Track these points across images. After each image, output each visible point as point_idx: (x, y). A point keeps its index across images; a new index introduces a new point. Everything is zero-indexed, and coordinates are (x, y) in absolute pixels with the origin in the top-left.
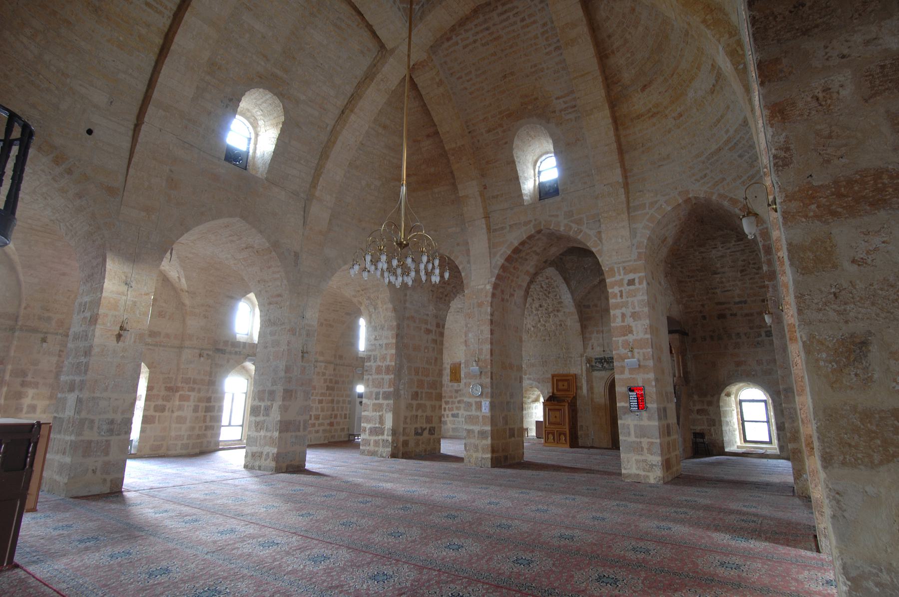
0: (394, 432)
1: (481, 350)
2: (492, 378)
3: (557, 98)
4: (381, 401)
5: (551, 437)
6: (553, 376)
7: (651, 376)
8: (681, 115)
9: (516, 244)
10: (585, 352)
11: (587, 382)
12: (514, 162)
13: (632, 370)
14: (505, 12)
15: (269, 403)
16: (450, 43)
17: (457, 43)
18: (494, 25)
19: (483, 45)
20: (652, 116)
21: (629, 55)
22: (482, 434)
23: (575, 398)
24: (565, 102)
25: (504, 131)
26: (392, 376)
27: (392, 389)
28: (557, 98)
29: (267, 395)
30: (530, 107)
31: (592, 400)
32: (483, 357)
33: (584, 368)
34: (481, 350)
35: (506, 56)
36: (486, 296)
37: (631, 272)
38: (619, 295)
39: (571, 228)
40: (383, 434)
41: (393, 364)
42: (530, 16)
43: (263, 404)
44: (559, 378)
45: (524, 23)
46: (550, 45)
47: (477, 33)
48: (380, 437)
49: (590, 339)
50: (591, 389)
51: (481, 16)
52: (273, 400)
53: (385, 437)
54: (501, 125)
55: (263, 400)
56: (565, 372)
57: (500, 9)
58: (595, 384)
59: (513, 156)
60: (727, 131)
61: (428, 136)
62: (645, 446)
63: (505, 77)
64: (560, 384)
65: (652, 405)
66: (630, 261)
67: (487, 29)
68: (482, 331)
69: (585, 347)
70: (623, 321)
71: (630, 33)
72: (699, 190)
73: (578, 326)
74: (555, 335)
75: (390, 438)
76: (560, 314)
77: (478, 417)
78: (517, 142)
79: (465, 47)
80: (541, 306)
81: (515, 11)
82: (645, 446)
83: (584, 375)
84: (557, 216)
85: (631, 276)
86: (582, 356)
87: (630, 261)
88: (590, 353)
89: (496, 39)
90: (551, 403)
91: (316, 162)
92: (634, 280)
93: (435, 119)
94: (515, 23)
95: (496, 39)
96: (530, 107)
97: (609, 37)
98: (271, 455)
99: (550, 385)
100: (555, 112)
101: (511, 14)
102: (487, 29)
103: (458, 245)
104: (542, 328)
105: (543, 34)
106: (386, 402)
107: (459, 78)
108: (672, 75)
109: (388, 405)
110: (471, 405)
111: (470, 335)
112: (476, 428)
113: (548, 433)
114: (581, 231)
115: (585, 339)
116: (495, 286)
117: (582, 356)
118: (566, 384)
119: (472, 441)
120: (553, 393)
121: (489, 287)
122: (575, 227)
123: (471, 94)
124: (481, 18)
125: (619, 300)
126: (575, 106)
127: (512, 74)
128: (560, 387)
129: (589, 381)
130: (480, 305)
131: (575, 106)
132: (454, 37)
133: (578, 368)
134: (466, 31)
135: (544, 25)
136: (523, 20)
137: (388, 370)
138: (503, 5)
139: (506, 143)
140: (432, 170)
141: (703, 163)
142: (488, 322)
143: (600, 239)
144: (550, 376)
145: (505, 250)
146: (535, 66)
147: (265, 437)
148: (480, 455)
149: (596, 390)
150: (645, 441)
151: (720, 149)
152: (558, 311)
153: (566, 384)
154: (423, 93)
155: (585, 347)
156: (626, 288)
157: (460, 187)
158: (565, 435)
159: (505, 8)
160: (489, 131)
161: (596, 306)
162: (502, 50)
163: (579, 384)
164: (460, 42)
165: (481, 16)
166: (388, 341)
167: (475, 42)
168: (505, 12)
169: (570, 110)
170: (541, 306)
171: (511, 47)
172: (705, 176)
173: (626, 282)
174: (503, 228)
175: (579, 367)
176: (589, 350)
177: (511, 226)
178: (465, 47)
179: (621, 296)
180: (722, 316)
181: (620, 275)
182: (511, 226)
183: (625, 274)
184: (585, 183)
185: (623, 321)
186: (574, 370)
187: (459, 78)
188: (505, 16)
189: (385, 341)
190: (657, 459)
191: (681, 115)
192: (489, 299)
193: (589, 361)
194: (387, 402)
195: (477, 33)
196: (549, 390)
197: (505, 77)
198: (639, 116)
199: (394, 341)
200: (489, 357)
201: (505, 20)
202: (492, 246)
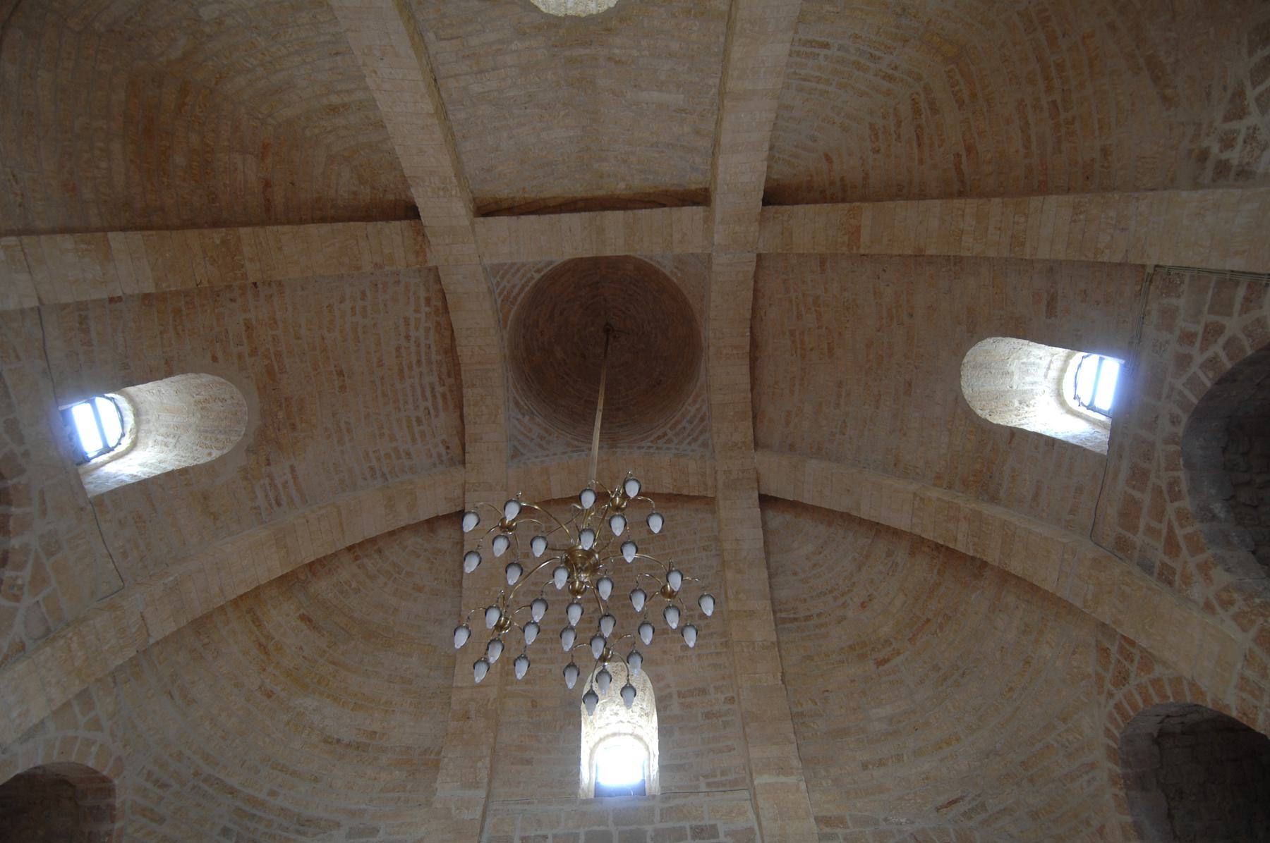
3: (292, 468)
8: (270, 695)
12: (169, 374)
14: (434, 397)
16: (422, 302)
17: (417, 311)
18: (421, 374)
19: (398, 349)
20: (260, 645)
21: (354, 585)
24: (285, 483)
25: (240, 356)
28: (292, 468)
30: (281, 415)
35: (373, 382)
39: (20, 567)
42: (423, 434)
45: (415, 423)
46: (379, 459)
47: (418, 346)
51: (439, 358)
54: (254, 352)
57: (439, 389)
59: (183, 371)
60: (273, 793)
61: (267, 184)
63: (341, 374)
67: (419, 362)
71: (385, 584)
72: (125, 795)
78: (206, 378)
79: (407, 320)
81: (432, 411)
84: (44, 513)
89: (401, 371)
93: (312, 229)
94: (417, 407)
95: (401, 371)
96: (281, 415)
97: (379, 551)
100: (269, 464)
101: (429, 404)
102: (419, 362)
105: (396, 450)
107: (364, 294)
108: (334, 663)
114: (17, 598)
123: (330, 307)
124: (434, 357)
126: (279, 505)
127: (343, 388)
131: (279, 505)
132: (427, 309)
134: (427, 330)
135: (408, 454)
136: (419, 421)
138: (444, 396)
139: (215, 359)
140: (179, 159)
141: (196, 774)
146: (349, 431)
151: (232, 791)
154: (371, 227)
157: (137, 237)
159: (438, 396)
160: (248, 326)
162: (382, 378)
164: (418, 315)
165: (439, 358)
167: (408, 338)
168: (434, 397)
169: (271, 495)
171: (384, 395)
172: (163, 786)
178: (407, 320)
184: (125, 555)
187: (364, 294)
188: (428, 394)
191: (270, 695)
195: (418, 346)
197: (341, 374)
198: (257, 622)
201: (423, 392)
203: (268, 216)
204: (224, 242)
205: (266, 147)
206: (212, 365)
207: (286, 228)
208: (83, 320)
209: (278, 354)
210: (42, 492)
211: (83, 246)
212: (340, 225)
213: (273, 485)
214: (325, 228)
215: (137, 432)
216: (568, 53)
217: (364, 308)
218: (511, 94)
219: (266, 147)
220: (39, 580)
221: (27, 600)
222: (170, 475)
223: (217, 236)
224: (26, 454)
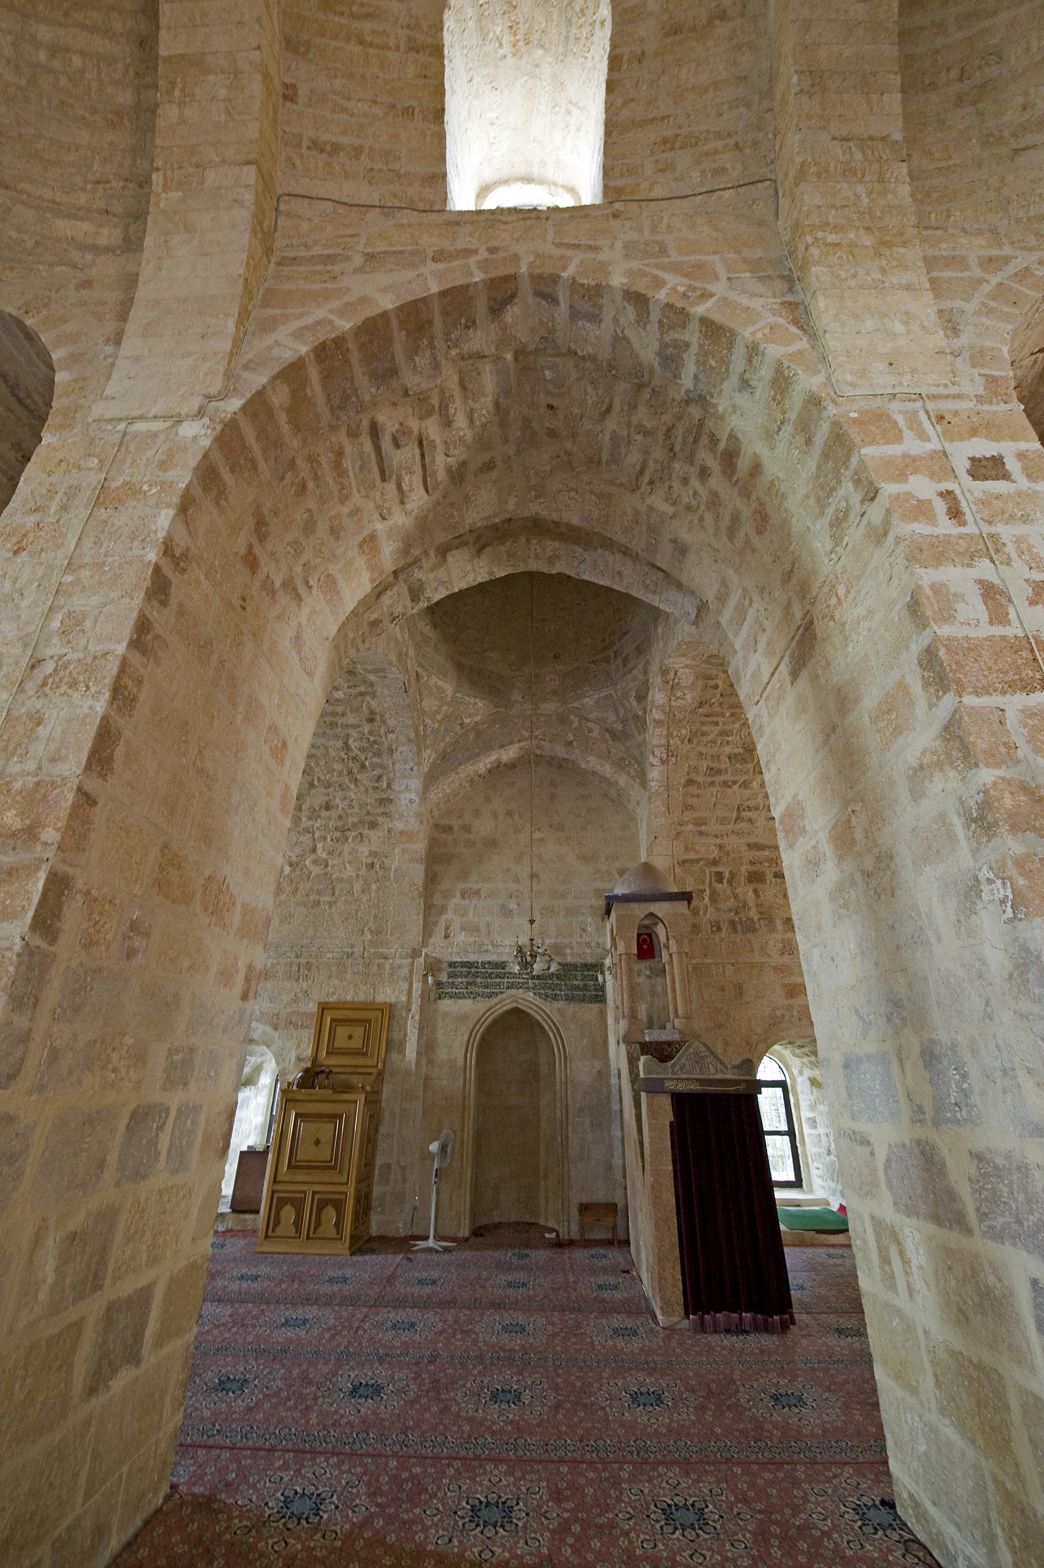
2: (46, 921)
5: (288, 1213)
6: (324, 1008)
10: (424, 944)
11: (421, 1030)
12: (438, 51)
23: (380, 1074)
31: (427, 1081)
33: (417, 986)
37: (974, 432)
38: (940, 507)
39: (659, 283)
44: (340, 1015)
49: (443, 909)
50: (428, 1048)
56: (361, 997)
58: (440, 1036)
59: (438, 27)
64: (342, 1031)
66: (958, 397)
68: (73, 625)
69: (428, 930)
70: (999, 617)
73: (418, 873)
74: (350, 892)
76: (373, 835)
80: (328, 807)
83: (415, 1008)
85: (983, 447)
86: (415, 953)
87: (958, 397)
88: (440, 948)
90: (309, 1089)
92: (997, 462)
99: (308, 1036)
104: (316, 870)
113: (282, 1202)
115: (431, 912)
116: (228, 438)
117: (415, 953)
118: (359, 1032)
120: (315, 1060)
121: (197, 434)
125: (945, 527)
128: (341, 1041)
129: (426, 1027)
133: (398, 989)
142: (135, 582)
144: (313, 1008)
149: (442, 1054)
152: (373, 825)
153: (359, 1032)
155: (428, 930)
156: (971, 491)
158: (338, 1206)
161: (467, 828)
163: (396, 1035)
170: (328, 807)
173: (961, 465)
175: (405, 986)
176: (437, 939)
179: (955, 513)
180: (756, 878)
181: (923, 436)
183: (949, 436)
185: (999, 617)
186: (386, 994)
192: (182, 477)
193: (432, 967)
196: (300, 1047)
200: (71, 767)
202: (258, 301)
210: (559, 245)
211: (177, 93)
215: (556, 185)
222: (611, 86)
224: (492, 250)
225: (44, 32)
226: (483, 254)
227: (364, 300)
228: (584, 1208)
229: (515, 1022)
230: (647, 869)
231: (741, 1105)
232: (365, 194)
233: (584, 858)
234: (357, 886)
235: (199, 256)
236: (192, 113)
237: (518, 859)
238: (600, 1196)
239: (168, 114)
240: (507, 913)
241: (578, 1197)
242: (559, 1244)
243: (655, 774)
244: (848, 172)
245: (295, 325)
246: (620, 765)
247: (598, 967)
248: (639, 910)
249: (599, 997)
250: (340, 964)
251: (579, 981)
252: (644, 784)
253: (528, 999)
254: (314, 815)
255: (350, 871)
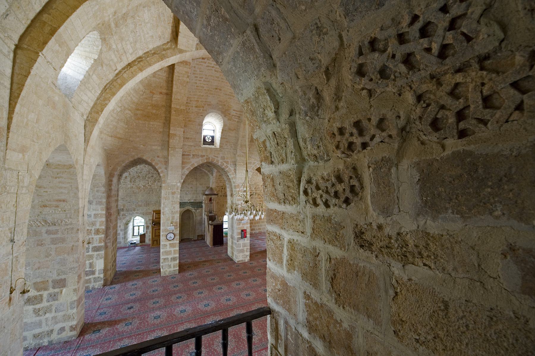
0: (105, 270)
1: (173, 218)
4: (91, 253)
7: (249, 225)
9: (196, 165)
13: (243, 224)
15: (57, 290)
17: (205, 63)
19: (215, 71)
22: (174, 259)
26: (103, 236)
27: (103, 244)
29: (51, 284)
30: (220, 107)
32: (174, 221)
34: (173, 218)
36: (177, 189)
39: (223, 164)
40: (93, 273)
41: (104, 227)
43: (45, 294)
48: (91, 277)
52: (64, 286)
53: (97, 275)
54: (203, 107)
55: (45, 289)
61: (161, 93)
62: (245, 250)
63: (216, 89)
65: (248, 236)
68: (174, 208)
75: (102, 276)
77: (171, 251)
82: (245, 250)
84: (217, 157)
91: (100, 92)
96: (220, 107)
98: (67, 329)
103: (158, 157)
104: (149, 187)
106: (96, 253)
109: (98, 255)
110: (167, 246)
111: (166, 209)
112: (170, 257)
119: (167, 263)
121: (179, 185)
122: (225, 164)
127: (220, 90)
130: (173, 193)
137: (97, 232)
140: (154, 111)
143: (235, 172)
145: (189, 167)
147: (54, 318)
148: (172, 269)
150: (245, 248)
157: (171, 128)
166: (97, 212)
174: (189, 155)
177: (193, 155)
182: (193, 155)
189: (93, 213)
190: (248, 253)
192: (179, 191)
194: (98, 253)
197: (216, 89)
199: (104, 212)
203: (169, 94)
204: (175, 111)
205: (151, 92)
206: (203, 117)
207: (173, 96)
208: (187, 138)
209: (205, 102)
212: (174, 82)
213: (235, 116)
214: (174, 86)
216: (114, 29)
217: (200, 77)
218: (132, 39)
219: (151, 92)
220: (227, 162)
221: (229, 166)
223: (173, 112)
225: (152, 123)
226: (206, 157)
227: (193, 164)
228: (198, 236)
229: (188, 211)
230: (211, 189)
231: (222, 225)
232: (192, 144)
233: (201, 184)
234: (158, 190)
235: (175, 160)
236: (174, 141)
237: (189, 184)
238: (200, 234)
239: (171, 141)
240: (186, 194)
241: (197, 234)
242: (195, 241)
243: (214, 175)
244: (243, 156)
245: (186, 168)
246: (209, 171)
247: (202, 203)
248: (210, 197)
249: (202, 207)
250: (155, 204)
251: (198, 205)
252: (212, 175)
253: (190, 208)
254: (149, 178)
255: (156, 187)
